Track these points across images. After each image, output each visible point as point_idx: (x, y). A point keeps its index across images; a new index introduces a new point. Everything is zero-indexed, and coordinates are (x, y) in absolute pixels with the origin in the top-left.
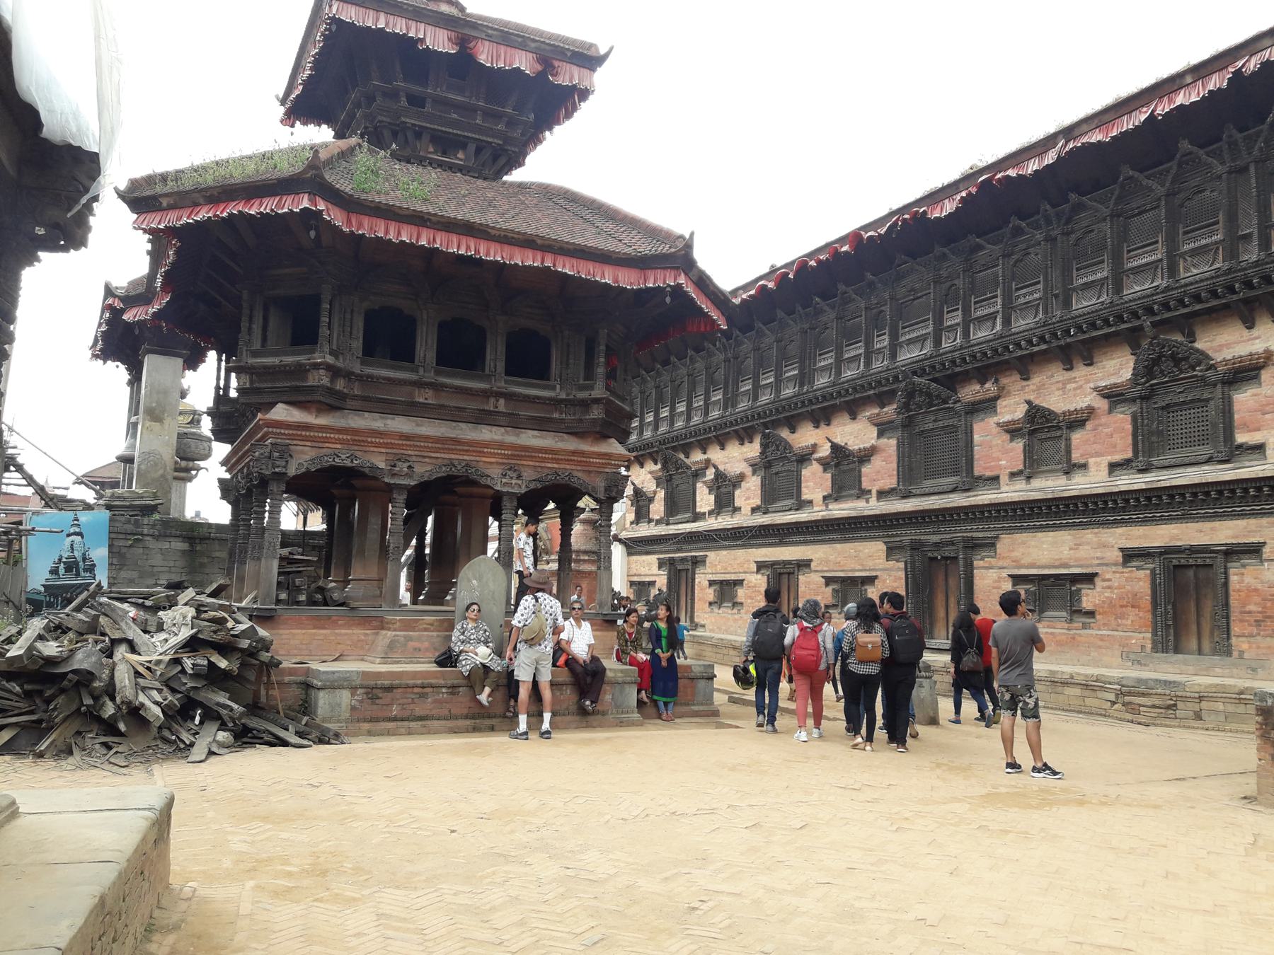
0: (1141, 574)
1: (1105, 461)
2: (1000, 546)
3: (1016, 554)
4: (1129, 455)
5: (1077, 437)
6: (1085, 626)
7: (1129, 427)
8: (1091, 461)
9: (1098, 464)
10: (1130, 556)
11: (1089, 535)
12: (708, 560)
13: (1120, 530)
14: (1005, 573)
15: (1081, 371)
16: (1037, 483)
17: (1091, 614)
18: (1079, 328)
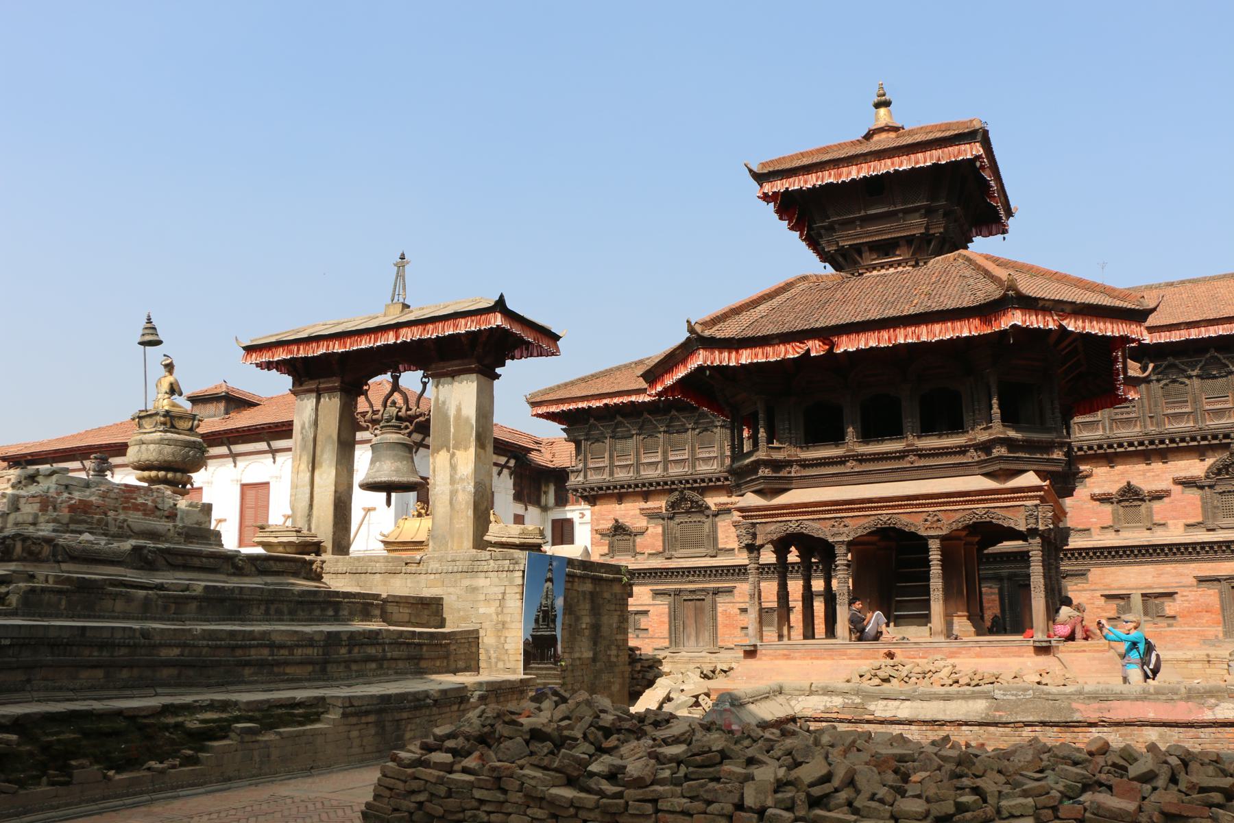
0: (1211, 592)
1: (1181, 522)
2: (1090, 576)
3: (1107, 581)
4: (1200, 520)
5: (1156, 505)
6: (1169, 625)
7: (1199, 503)
8: (1170, 522)
9: (1175, 525)
10: (1202, 580)
11: (1169, 568)
12: (736, 591)
13: (1193, 565)
14: (1098, 594)
15: (1157, 466)
16: (1123, 534)
17: (1173, 617)
18: (1172, 441)
